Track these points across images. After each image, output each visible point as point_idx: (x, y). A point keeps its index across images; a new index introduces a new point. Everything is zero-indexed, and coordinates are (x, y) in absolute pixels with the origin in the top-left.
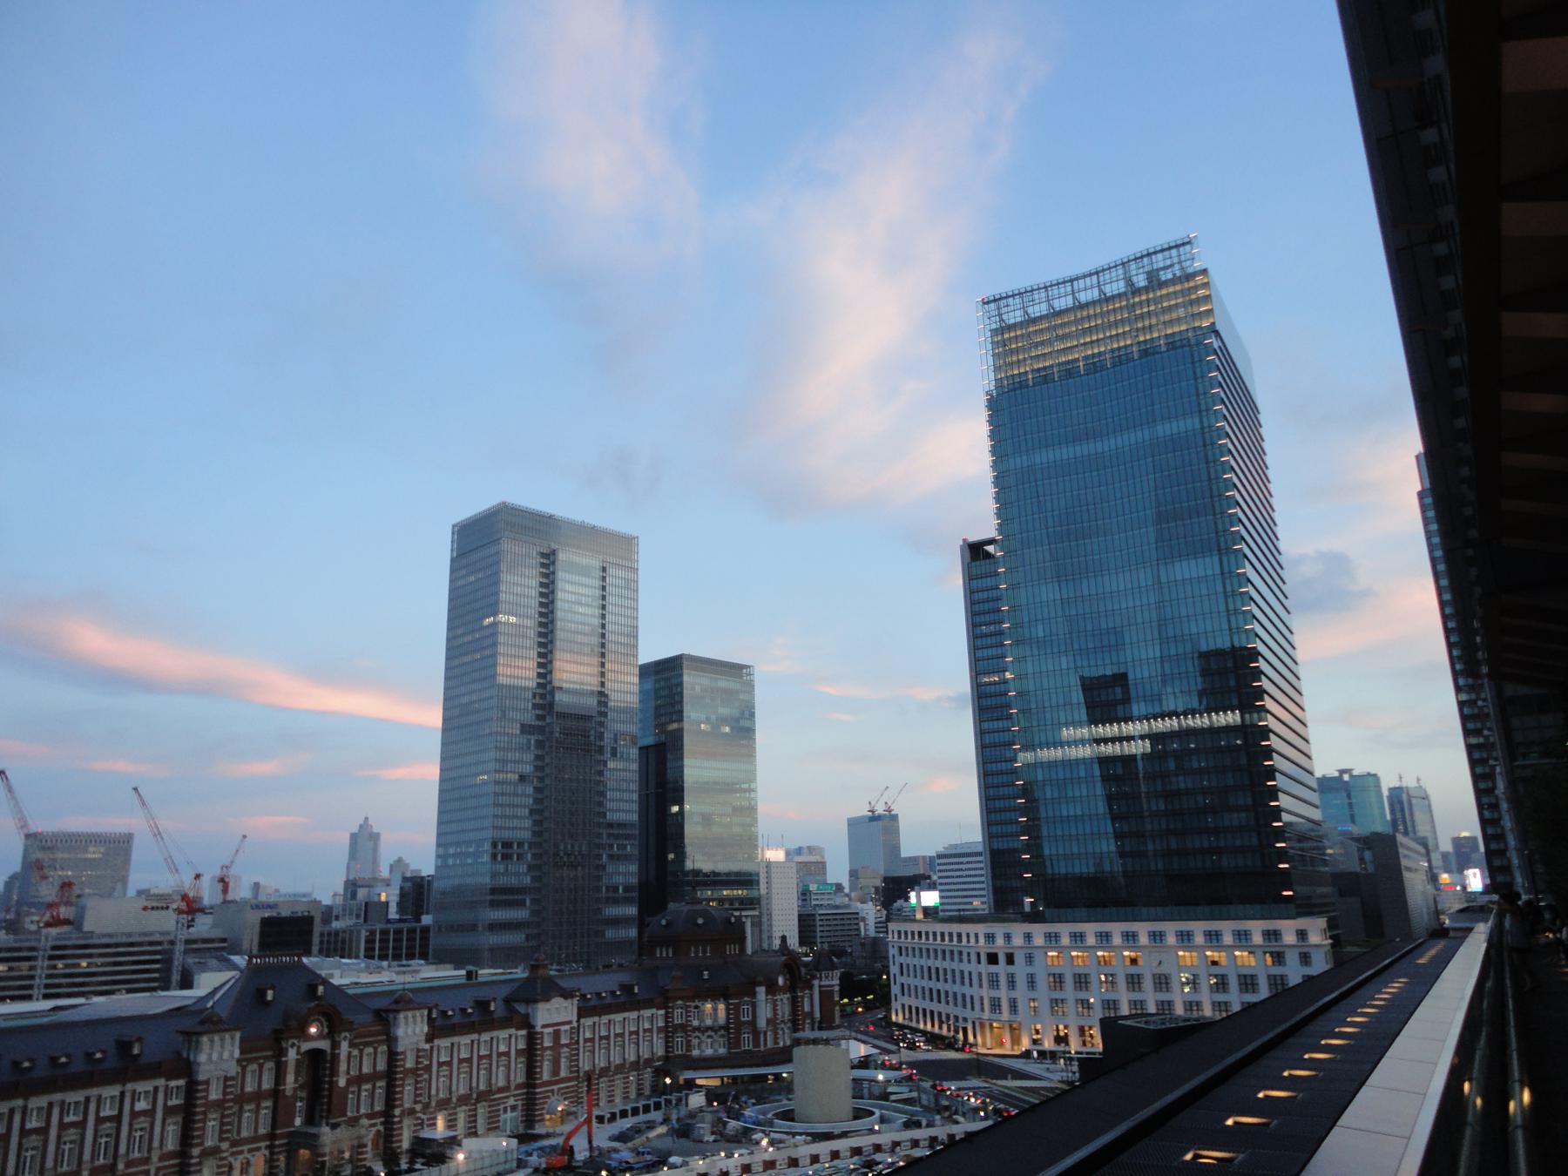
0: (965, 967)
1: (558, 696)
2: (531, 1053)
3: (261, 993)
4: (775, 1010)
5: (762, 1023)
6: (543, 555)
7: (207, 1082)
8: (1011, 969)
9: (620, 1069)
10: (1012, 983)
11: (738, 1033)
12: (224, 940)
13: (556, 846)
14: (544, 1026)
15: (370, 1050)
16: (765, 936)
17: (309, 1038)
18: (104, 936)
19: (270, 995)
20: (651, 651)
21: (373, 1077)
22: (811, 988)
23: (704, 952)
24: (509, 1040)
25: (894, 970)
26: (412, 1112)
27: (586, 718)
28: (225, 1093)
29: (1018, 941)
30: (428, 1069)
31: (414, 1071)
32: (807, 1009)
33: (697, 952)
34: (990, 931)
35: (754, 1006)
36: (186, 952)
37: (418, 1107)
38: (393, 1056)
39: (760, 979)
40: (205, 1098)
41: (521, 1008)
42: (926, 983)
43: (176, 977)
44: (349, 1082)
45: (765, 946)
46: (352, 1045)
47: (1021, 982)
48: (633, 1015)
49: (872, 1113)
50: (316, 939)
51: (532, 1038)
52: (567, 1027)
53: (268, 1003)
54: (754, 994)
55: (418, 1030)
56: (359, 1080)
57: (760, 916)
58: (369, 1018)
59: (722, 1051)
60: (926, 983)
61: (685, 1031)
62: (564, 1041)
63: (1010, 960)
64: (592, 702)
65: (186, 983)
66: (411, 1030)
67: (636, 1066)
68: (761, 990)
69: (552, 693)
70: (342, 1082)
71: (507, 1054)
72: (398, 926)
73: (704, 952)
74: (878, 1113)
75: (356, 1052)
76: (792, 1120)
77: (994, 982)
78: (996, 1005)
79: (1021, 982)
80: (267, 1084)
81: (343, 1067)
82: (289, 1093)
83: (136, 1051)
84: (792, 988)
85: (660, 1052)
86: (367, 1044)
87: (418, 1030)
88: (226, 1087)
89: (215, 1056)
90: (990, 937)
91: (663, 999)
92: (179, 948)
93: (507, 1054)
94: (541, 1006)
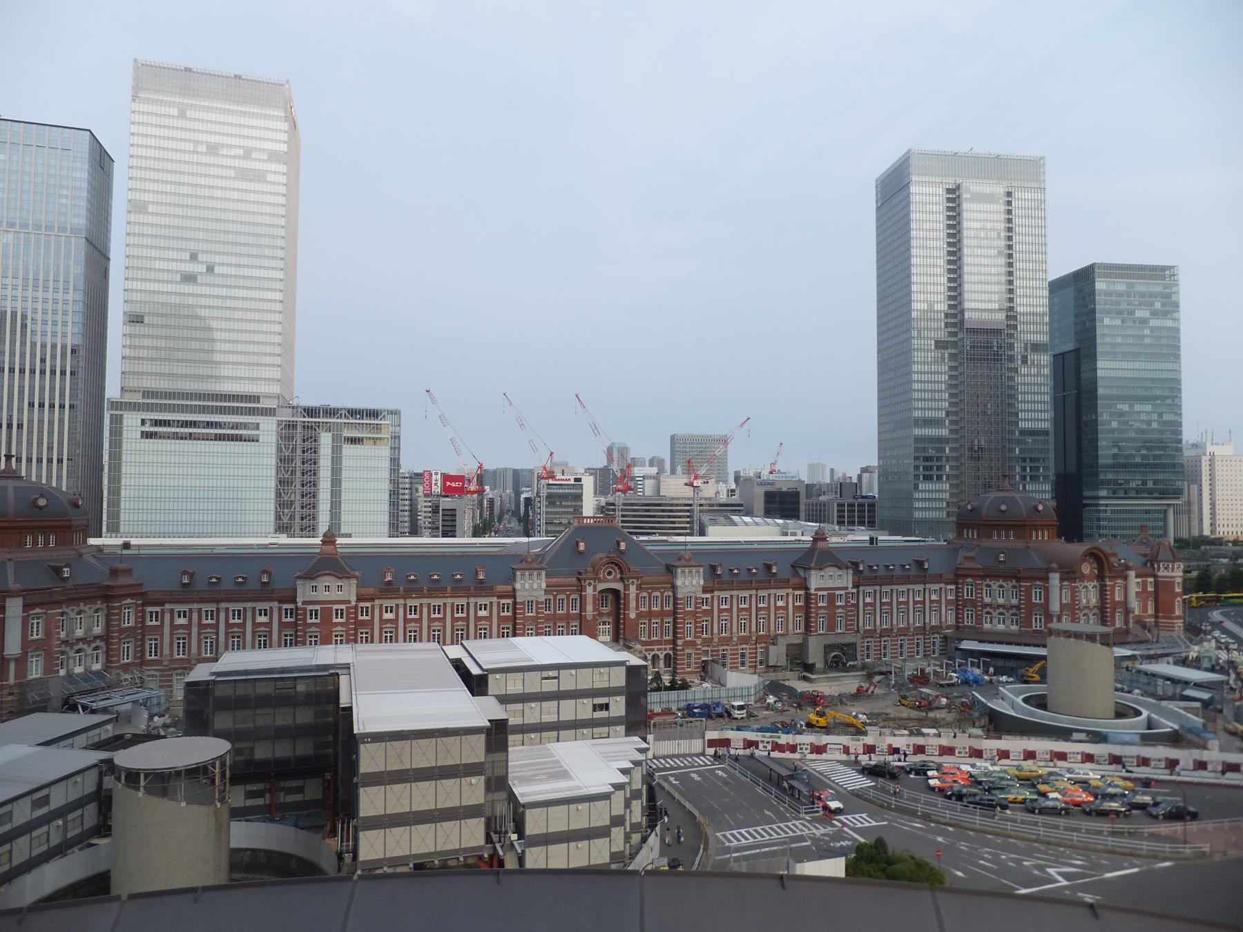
4: (1073, 597)
5: (1055, 607)
7: (523, 603)
9: (903, 632)
13: (972, 441)
17: (605, 580)
19: (582, 546)
21: (662, 614)
22: (1126, 578)
23: (1007, 536)
24: (786, 600)
26: (693, 644)
33: (999, 536)
35: (1047, 590)
36: (701, 511)
37: (699, 641)
38: (675, 599)
39: (1055, 565)
41: (801, 573)
43: (696, 527)
44: (640, 615)
46: (639, 588)
48: (920, 587)
49: (1138, 713)
50: (802, 507)
51: (808, 597)
52: (843, 592)
53: (581, 553)
54: (1046, 579)
55: (694, 582)
56: (650, 615)
58: (662, 569)
59: (1015, 628)
61: (975, 606)
62: (839, 604)
66: (690, 583)
67: (922, 630)
68: (1055, 578)
70: (633, 615)
71: (786, 608)
73: (1007, 536)
74: (1145, 713)
75: (645, 594)
81: (633, 604)
82: (589, 618)
84: (1101, 577)
85: (950, 619)
86: (654, 589)
87: (694, 582)
88: (538, 608)
89: (527, 586)
91: (957, 577)
92: (697, 508)
94: (813, 572)
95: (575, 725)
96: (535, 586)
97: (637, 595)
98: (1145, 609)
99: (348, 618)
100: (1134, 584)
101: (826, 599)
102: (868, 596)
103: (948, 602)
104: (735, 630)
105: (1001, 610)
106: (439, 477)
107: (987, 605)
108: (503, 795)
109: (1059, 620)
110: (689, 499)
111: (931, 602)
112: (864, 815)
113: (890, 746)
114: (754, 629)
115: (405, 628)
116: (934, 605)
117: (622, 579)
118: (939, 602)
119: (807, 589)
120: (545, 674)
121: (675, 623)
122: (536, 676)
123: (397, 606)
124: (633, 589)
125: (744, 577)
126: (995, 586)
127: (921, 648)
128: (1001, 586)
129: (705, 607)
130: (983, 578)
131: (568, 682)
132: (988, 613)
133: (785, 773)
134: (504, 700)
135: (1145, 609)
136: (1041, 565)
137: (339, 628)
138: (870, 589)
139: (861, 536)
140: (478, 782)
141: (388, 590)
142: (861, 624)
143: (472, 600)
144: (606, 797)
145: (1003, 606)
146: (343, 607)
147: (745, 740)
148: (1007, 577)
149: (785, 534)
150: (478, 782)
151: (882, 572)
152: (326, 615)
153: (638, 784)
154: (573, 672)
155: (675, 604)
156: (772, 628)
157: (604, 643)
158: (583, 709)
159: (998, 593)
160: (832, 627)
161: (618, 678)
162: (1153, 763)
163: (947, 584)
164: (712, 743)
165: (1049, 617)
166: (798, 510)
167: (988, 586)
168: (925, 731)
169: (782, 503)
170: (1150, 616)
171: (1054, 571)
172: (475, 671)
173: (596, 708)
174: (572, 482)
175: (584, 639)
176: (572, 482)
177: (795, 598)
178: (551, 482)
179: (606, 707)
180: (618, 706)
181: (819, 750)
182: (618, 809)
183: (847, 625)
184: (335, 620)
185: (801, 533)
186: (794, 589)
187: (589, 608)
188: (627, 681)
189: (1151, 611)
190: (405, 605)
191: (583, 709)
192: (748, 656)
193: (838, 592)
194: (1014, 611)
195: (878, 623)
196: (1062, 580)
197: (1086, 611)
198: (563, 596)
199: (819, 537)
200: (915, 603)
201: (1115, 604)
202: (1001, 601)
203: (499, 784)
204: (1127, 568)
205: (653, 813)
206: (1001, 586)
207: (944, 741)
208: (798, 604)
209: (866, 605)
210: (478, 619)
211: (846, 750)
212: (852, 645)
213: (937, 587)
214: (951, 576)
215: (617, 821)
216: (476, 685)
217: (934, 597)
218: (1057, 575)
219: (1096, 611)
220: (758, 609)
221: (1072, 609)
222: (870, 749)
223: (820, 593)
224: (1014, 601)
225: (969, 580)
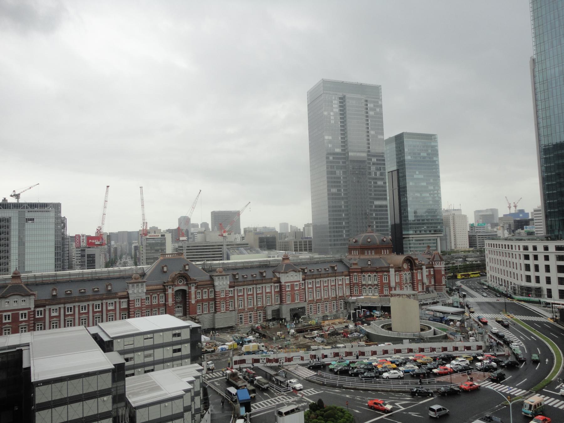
0: (514, 260)
1: (350, 154)
2: (280, 293)
3: (163, 268)
4: (400, 279)
5: (393, 284)
6: (340, 98)
7: (134, 301)
8: (536, 262)
9: (326, 300)
10: (537, 268)
11: (382, 288)
12: (247, 244)
14: (285, 283)
15: (206, 290)
16: (448, 244)
17: (178, 285)
18: (213, 243)
19: (165, 269)
20: (389, 132)
21: (209, 300)
22: (422, 269)
23: (371, 253)
25: (487, 260)
27: (363, 162)
28: (142, 305)
29: (540, 248)
30: (233, 297)
31: (225, 298)
32: (419, 278)
33: (368, 253)
34: (526, 244)
35: (389, 276)
38: (215, 292)
39: (392, 265)
40: (134, 306)
41: (277, 275)
42: (498, 266)
43: (225, 256)
44: (197, 302)
45: (453, 248)
46: (197, 288)
47: (542, 268)
48: (334, 278)
49: (430, 328)
50: (277, 244)
51: (281, 287)
52: (298, 283)
53: (165, 272)
54: (389, 272)
55: (225, 283)
56: (203, 300)
57: (446, 235)
60: (498, 266)
62: (296, 289)
63: (536, 258)
64: (364, 155)
65: (228, 258)
67: (335, 298)
68: (392, 271)
69: (348, 153)
70: (193, 302)
71: (271, 293)
72: (304, 240)
73: (371, 253)
75: (199, 291)
76: (390, 329)
77: (528, 267)
78: (528, 279)
79: (542, 268)
80: (162, 301)
81: (193, 296)
82: (170, 305)
83: (109, 288)
84: (411, 269)
87: (225, 283)
88: (142, 302)
90: (526, 248)
91: (350, 272)
92: (225, 247)
93: (271, 293)
95: (163, 361)
96: (140, 291)
97: (195, 291)
98: (430, 283)
99: (29, 318)
100: (425, 271)
101: (290, 287)
102: (310, 284)
103: (346, 284)
104: (246, 305)
105: (370, 287)
106: (85, 238)
107: (363, 285)
108: (123, 404)
109: (395, 290)
110: (221, 242)
111: (339, 285)
112: (312, 389)
113: (323, 354)
114: (255, 304)
115: (65, 320)
116: (340, 286)
117: (187, 284)
118: (342, 285)
119: (280, 282)
120: (146, 336)
121: (215, 304)
122: (142, 337)
123: (60, 308)
124: (193, 289)
125: (250, 278)
126: (367, 275)
127: (335, 306)
128: (369, 276)
129: (230, 295)
130: (362, 272)
131: (158, 339)
132: (364, 288)
133: (273, 373)
134: (122, 353)
135: (430, 283)
136: (386, 265)
137: (24, 324)
138: (310, 281)
139: (305, 256)
140: (108, 399)
141: (54, 300)
142: (307, 298)
143: (104, 301)
144: (181, 397)
145: (371, 285)
146: (26, 312)
147: (253, 359)
148: (372, 272)
149: (270, 257)
150: (108, 399)
151: (316, 272)
152: (15, 318)
153: (198, 388)
154: (161, 334)
155: (215, 294)
156: (264, 303)
157: (178, 317)
158: (168, 352)
159: (370, 279)
160: (293, 300)
161: (186, 335)
162: (437, 350)
163: (345, 276)
164: (236, 363)
165: (390, 289)
166: (275, 245)
167: (364, 276)
168: (338, 345)
169: (268, 242)
170: (432, 285)
171: (392, 268)
172: (106, 339)
173: (175, 351)
174: (160, 237)
175: (167, 316)
176: (160, 237)
177: (275, 287)
178: (148, 237)
179: (179, 350)
180: (186, 349)
181: (289, 360)
182: (187, 402)
183: (300, 299)
184: (21, 320)
185: (276, 256)
186: (274, 283)
187: (170, 301)
188: (191, 336)
189: (433, 283)
190: (65, 308)
191: (168, 352)
192: (253, 317)
193: (295, 283)
194: (376, 286)
195: (315, 297)
196: (395, 271)
197: (406, 285)
198: (156, 295)
199: (286, 258)
200: (332, 286)
201: (418, 280)
202: (370, 283)
203: (120, 398)
204: (423, 265)
205: (206, 403)
206: (369, 276)
207: (347, 350)
208: (276, 290)
209: (309, 288)
210: (108, 311)
211: (302, 359)
212: (303, 308)
213: (341, 278)
214: (347, 273)
215: (187, 409)
216: (106, 346)
217: (340, 283)
218: (393, 270)
219: (410, 284)
220: (257, 294)
221: (400, 285)
222: (314, 357)
223: (287, 284)
224: (376, 282)
225: (355, 274)
